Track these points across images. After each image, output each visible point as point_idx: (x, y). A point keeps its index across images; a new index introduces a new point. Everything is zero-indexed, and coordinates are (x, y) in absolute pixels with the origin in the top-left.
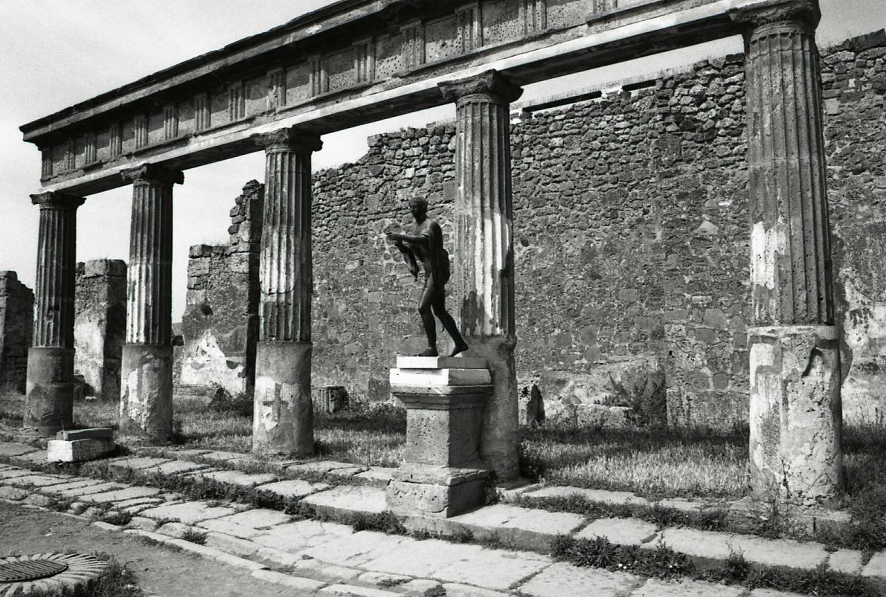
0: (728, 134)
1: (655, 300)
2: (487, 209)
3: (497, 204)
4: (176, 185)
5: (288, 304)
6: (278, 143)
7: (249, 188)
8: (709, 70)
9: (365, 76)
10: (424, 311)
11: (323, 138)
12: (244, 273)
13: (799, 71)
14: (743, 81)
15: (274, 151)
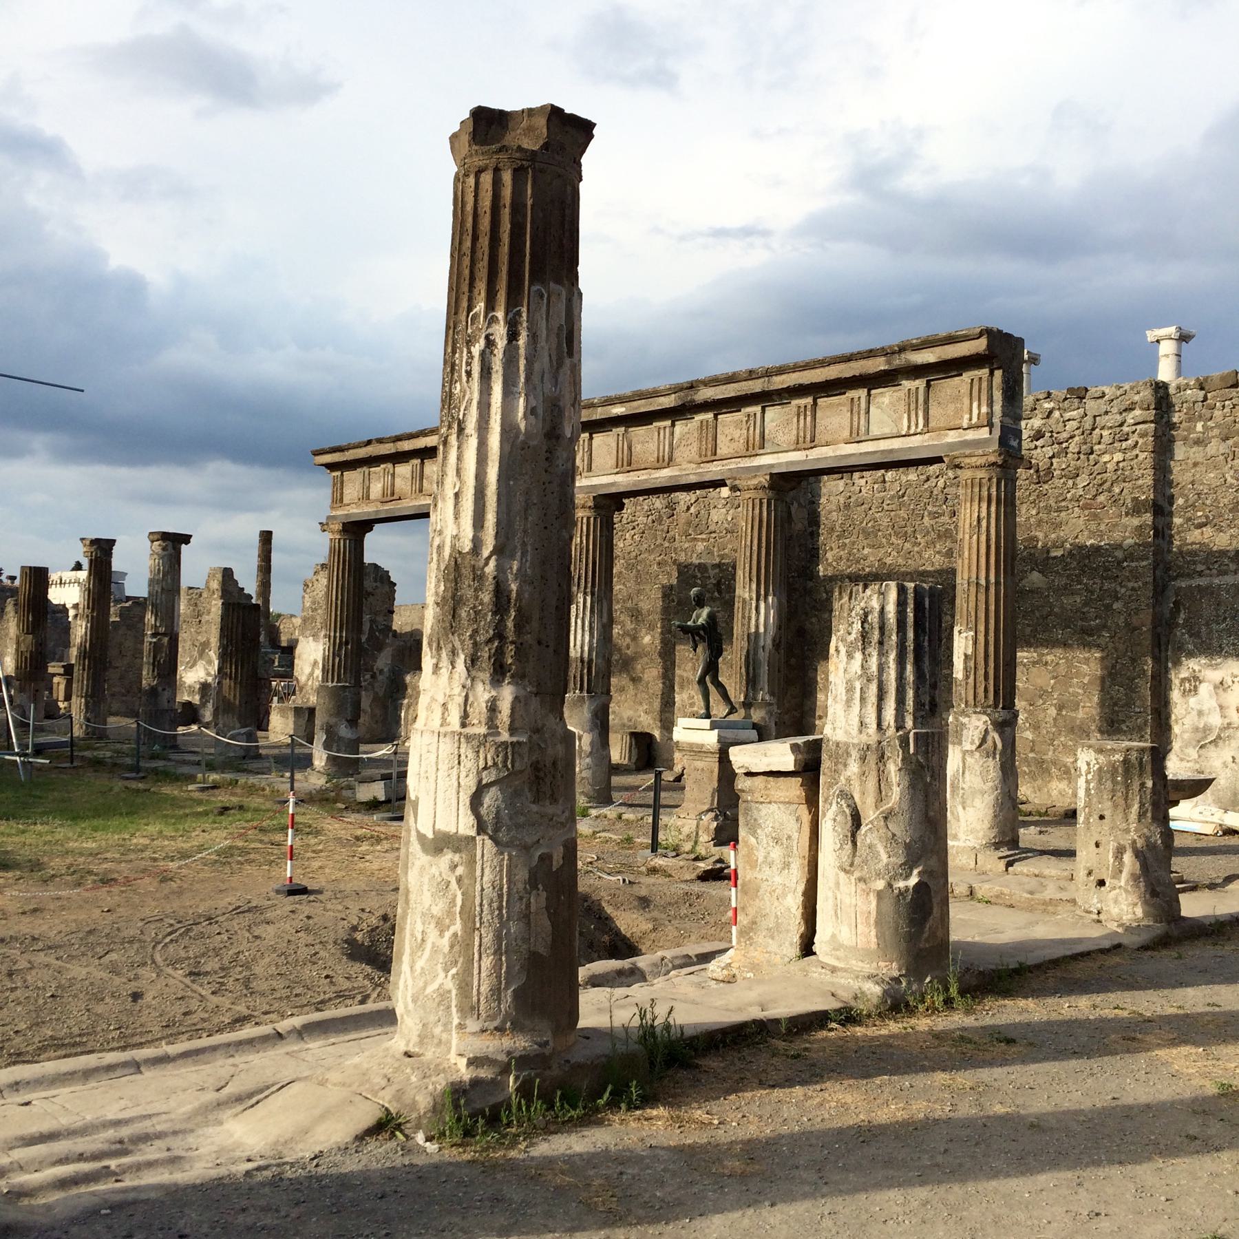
0: (1065, 476)
5: (590, 661)
10: (702, 682)
13: (993, 509)
14: (1083, 417)
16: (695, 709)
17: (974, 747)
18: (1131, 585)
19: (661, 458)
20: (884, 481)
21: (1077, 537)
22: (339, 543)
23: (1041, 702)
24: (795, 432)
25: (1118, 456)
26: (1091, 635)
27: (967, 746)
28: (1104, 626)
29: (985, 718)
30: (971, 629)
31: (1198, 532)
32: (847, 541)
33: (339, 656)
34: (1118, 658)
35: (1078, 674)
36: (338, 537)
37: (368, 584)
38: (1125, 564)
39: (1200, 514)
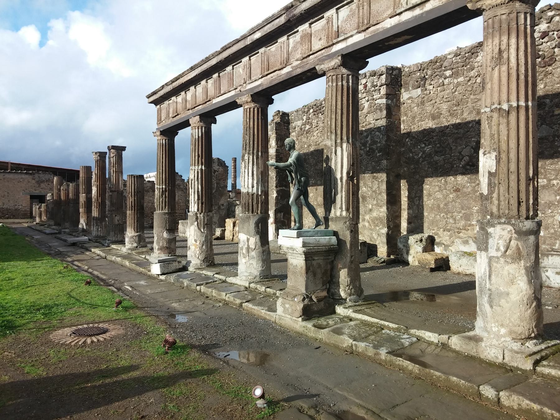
2: (339, 141)
3: (345, 138)
4: (213, 125)
7: (275, 115)
8: (551, 11)
9: (284, 60)
11: (217, 117)
17: (499, 254)
19: (282, 62)
20: (444, 85)
23: (550, 211)
24: (357, 20)
27: (492, 252)
29: (510, 228)
30: (495, 150)
36: (160, 138)
37: (215, 167)
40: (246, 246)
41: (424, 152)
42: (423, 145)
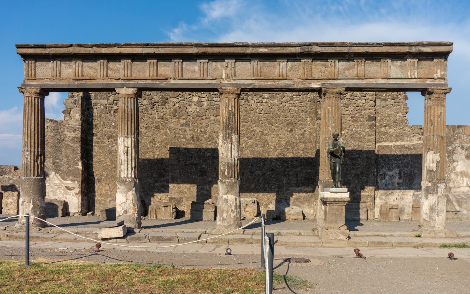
1: (308, 166)
6: (233, 93)
12: (76, 137)
15: (231, 97)
16: (181, 189)
18: (368, 144)
21: (349, 127)
22: (35, 99)
25: (363, 101)
26: (354, 160)
28: (359, 157)
31: (384, 128)
32: (246, 124)
33: (37, 162)
34: (364, 168)
35: (350, 173)
38: (366, 137)
39: (385, 123)
40: (235, 204)
41: (247, 143)
42: (247, 139)
